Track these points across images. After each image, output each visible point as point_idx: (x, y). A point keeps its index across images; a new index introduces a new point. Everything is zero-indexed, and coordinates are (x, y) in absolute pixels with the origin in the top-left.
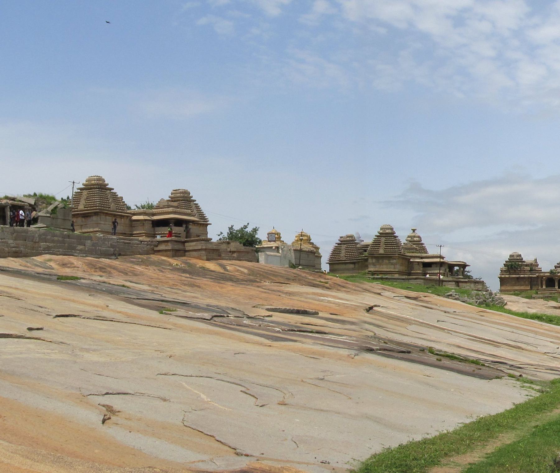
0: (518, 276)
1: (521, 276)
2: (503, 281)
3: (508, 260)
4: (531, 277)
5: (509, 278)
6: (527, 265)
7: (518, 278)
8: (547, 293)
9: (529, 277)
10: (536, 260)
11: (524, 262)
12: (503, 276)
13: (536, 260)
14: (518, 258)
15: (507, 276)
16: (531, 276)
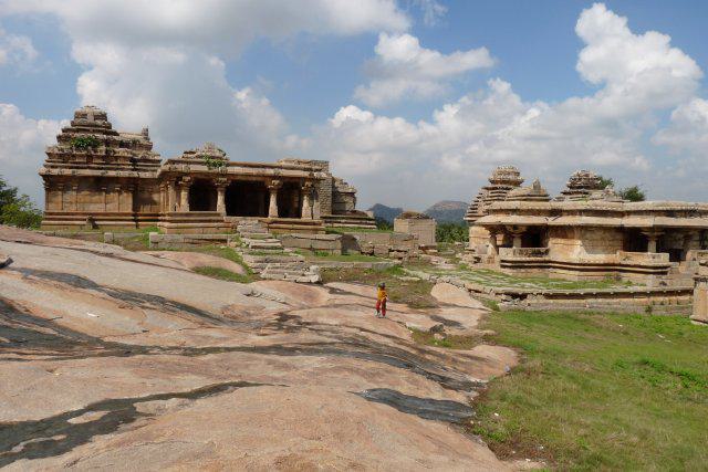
0: (98, 173)
1: (112, 173)
2: (52, 184)
3: (69, 126)
4: (138, 178)
5: (72, 178)
6: (122, 144)
7: (98, 179)
8: (197, 230)
9: (130, 180)
10: (146, 133)
11: (116, 134)
12: (55, 172)
13: (146, 133)
14: (99, 122)
15: (68, 172)
16: (135, 174)
